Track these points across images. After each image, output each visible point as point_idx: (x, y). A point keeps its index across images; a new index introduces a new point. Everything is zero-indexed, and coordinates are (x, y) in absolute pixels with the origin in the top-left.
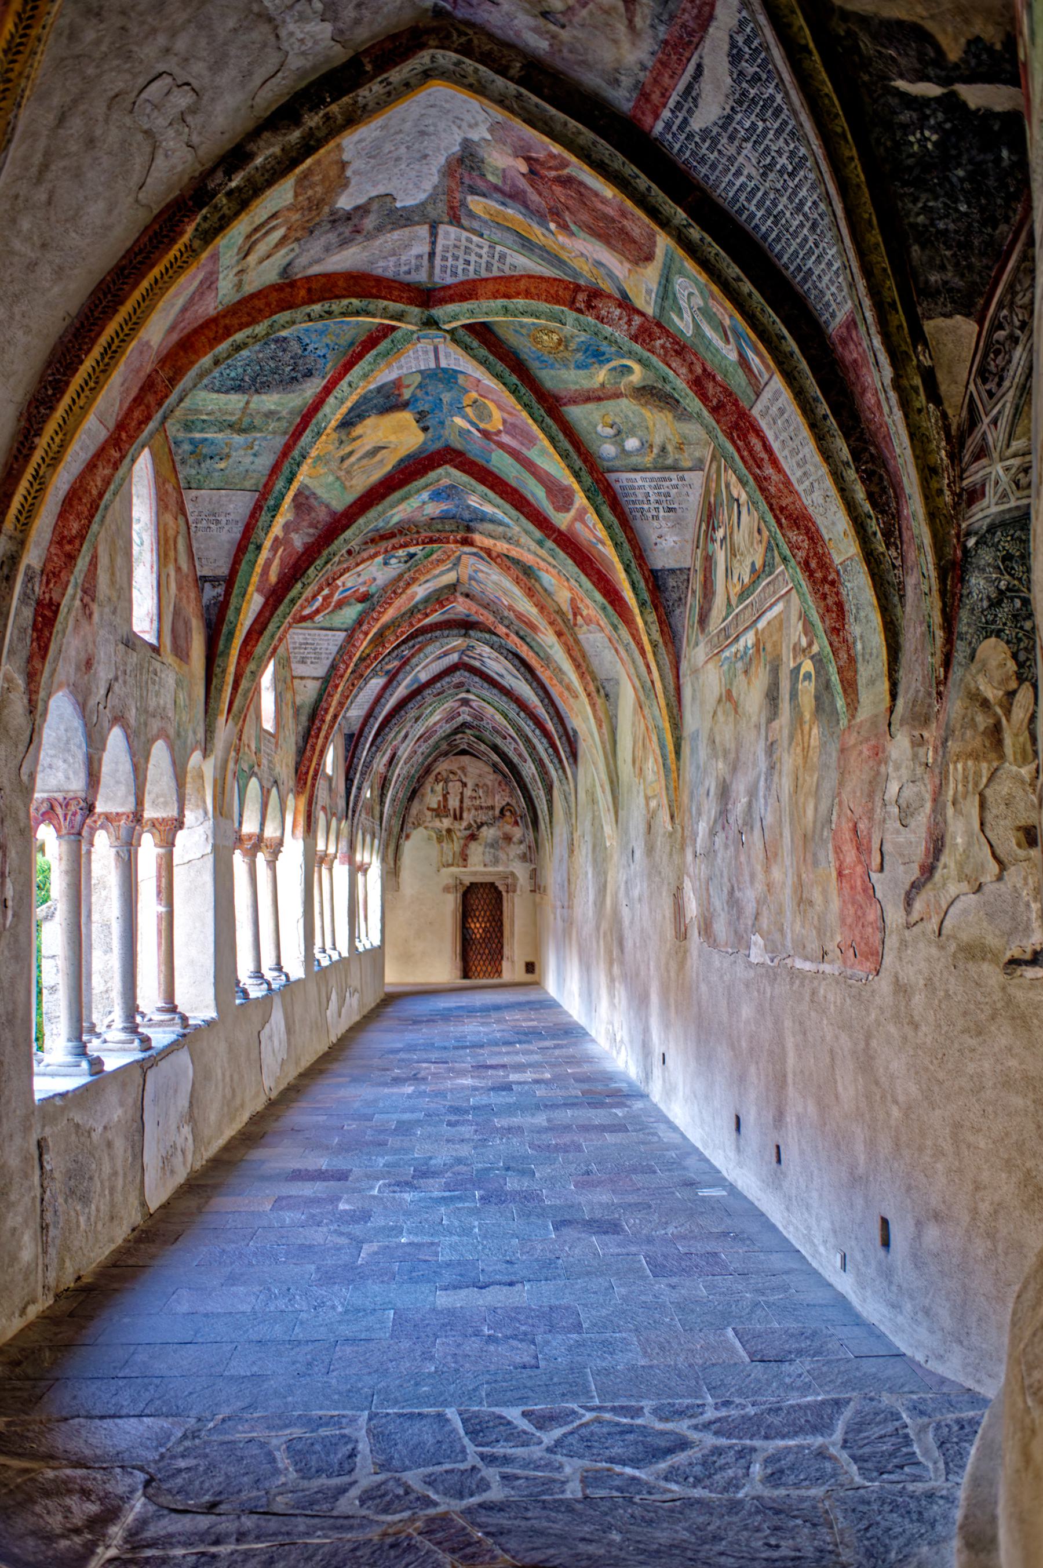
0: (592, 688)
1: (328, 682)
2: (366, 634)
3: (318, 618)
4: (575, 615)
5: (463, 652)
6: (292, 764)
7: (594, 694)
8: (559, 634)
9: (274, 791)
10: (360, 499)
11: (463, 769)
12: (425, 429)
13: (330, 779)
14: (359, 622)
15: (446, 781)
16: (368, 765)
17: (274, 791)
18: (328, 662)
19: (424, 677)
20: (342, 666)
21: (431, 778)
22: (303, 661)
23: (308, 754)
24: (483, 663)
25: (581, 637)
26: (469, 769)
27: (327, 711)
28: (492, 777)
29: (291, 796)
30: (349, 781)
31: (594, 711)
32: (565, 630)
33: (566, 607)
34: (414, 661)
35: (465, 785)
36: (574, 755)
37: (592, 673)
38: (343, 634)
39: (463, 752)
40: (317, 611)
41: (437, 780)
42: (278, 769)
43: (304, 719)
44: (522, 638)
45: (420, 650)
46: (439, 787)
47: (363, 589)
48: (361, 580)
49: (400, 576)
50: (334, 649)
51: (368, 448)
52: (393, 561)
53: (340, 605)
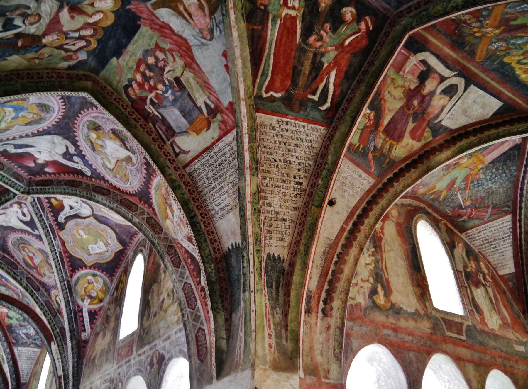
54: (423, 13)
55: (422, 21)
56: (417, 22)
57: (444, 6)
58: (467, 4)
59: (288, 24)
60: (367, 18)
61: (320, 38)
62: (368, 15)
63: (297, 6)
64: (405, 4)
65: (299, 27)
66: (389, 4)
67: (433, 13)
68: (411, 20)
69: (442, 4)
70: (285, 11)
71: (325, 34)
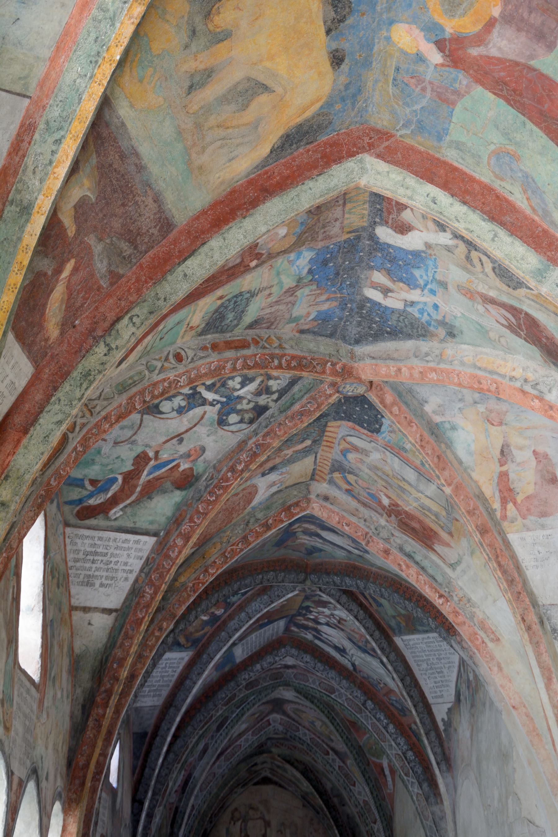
0: (532, 618)
1: (124, 616)
2: (187, 538)
3: (115, 512)
4: (504, 501)
5: (291, 621)
6: (63, 750)
7: (536, 627)
8: (483, 531)
9: (31, 787)
10: (214, 205)
12: (337, 59)
13: (113, 792)
14: (176, 520)
15: (245, 821)
16: (162, 780)
17: (31, 787)
18: (127, 586)
19: (240, 654)
20: (149, 591)
21: (226, 817)
22: (88, 583)
23: (89, 734)
24: (317, 633)
25: (513, 537)
27: (121, 662)
29: (57, 807)
30: (137, 802)
31: (538, 655)
32: (490, 524)
33: (490, 490)
34: (232, 624)
35: (268, 824)
36: (446, 760)
37: (531, 595)
38: (151, 541)
39: (266, 781)
40: (114, 501)
41: (233, 819)
42: (40, 750)
43: (85, 676)
44: (409, 556)
45: (241, 608)
47: (184, 466)
48: (183, 449)
49: (241, 445)
50: (137, 565)
51: (235, 75)
52: (233, 418)
53: (150, 490)
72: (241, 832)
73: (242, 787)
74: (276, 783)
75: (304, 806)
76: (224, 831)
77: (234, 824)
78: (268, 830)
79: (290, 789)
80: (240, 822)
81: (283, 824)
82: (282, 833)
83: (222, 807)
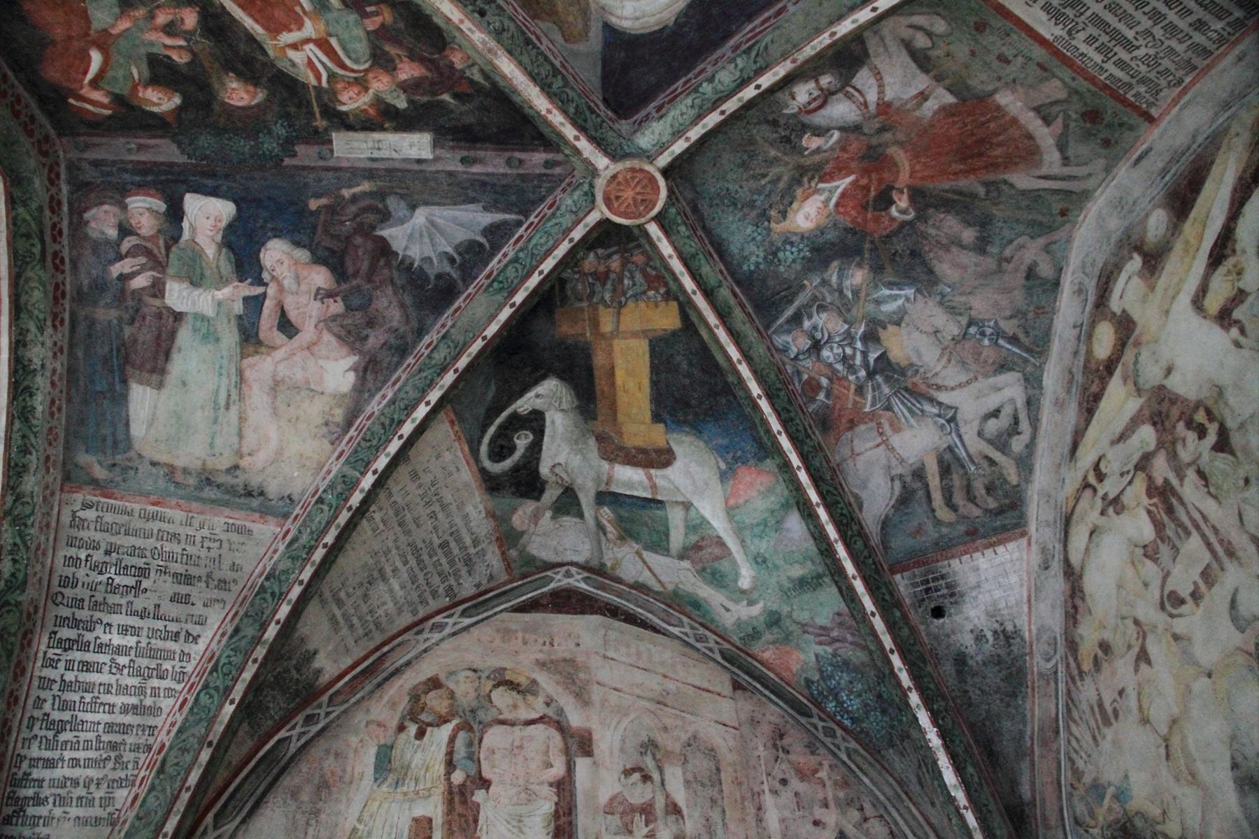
11: (570, 672)
15: (472, 724)
21: (385, 706)
26: (605, 673)
28: (729, 708)
35: (580, 744)
39: (568, 602)
41: (417, 717)
46: (428, 755)
54: (39, 247)
55: (23, 235)
56: (24, 220)
57: (36, 312)
58: (21, 372)
59: (279, 14)
60: (108, 112)
61: (170, 29)
62: (110, 117)
63: (292, 54)
64: (71, 193)
65: (248, 22)
66: (96, 164)
67: (31, 274)
68: (34, 206)
69: (42, 307)
70: (309, 29)
71: (169, 42)
72: (450, 765)
73: (464, 614)
74: (613, 612)
75: (737, 686)
76: (369, 757)
77: (420, 734)
78: (582, 764)
79: (676, 631)
80: (447, 730)
81: (650, 746)
82: (646, 778)
83: (369, 672)
